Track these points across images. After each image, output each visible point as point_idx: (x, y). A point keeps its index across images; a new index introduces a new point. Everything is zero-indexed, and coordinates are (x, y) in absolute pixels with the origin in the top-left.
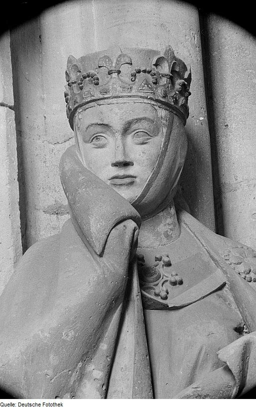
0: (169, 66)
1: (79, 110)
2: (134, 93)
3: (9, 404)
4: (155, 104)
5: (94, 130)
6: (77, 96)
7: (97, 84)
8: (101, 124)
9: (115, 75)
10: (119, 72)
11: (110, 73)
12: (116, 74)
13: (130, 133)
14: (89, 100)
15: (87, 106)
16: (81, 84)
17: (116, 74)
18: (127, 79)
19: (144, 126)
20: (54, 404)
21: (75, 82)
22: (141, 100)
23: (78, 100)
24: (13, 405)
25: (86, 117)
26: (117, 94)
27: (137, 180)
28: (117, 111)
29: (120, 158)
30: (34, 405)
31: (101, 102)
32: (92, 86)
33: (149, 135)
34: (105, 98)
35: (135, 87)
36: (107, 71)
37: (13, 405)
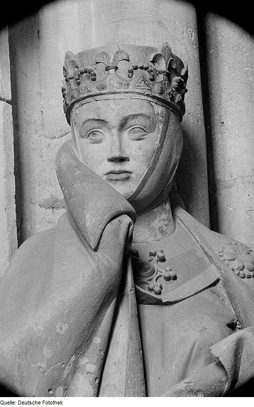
0: (166, 63)
1: (77, 105)
2: (130, 89)
3: (9, 402)
4: (152, 100)
5: (90, 125)
6: (74, 91)
7: (94, 80)
8: (98, 120)
9: (112, 71)
10: (116, 68)
11: (107, 69)
12: (114, 70)
13: (127, 129)
14: (86, 95)
15: (84, 101)
16: (79, 79)
17: (114, 70)
19: (139, 122)
20: (54, 403)
21: (73, 78)
22: (138, 96)
23: (75, 96)
24: (13, 403)
25: (82, 113)
26: (113, 90)
27: (133, 175)
28: (114, 106)
29: (116, 154)
30: (34, 403)
31: (98, 98)
32: (89, 82)
33: (145, 131)
35: (131, 83)
37: (13, 403)
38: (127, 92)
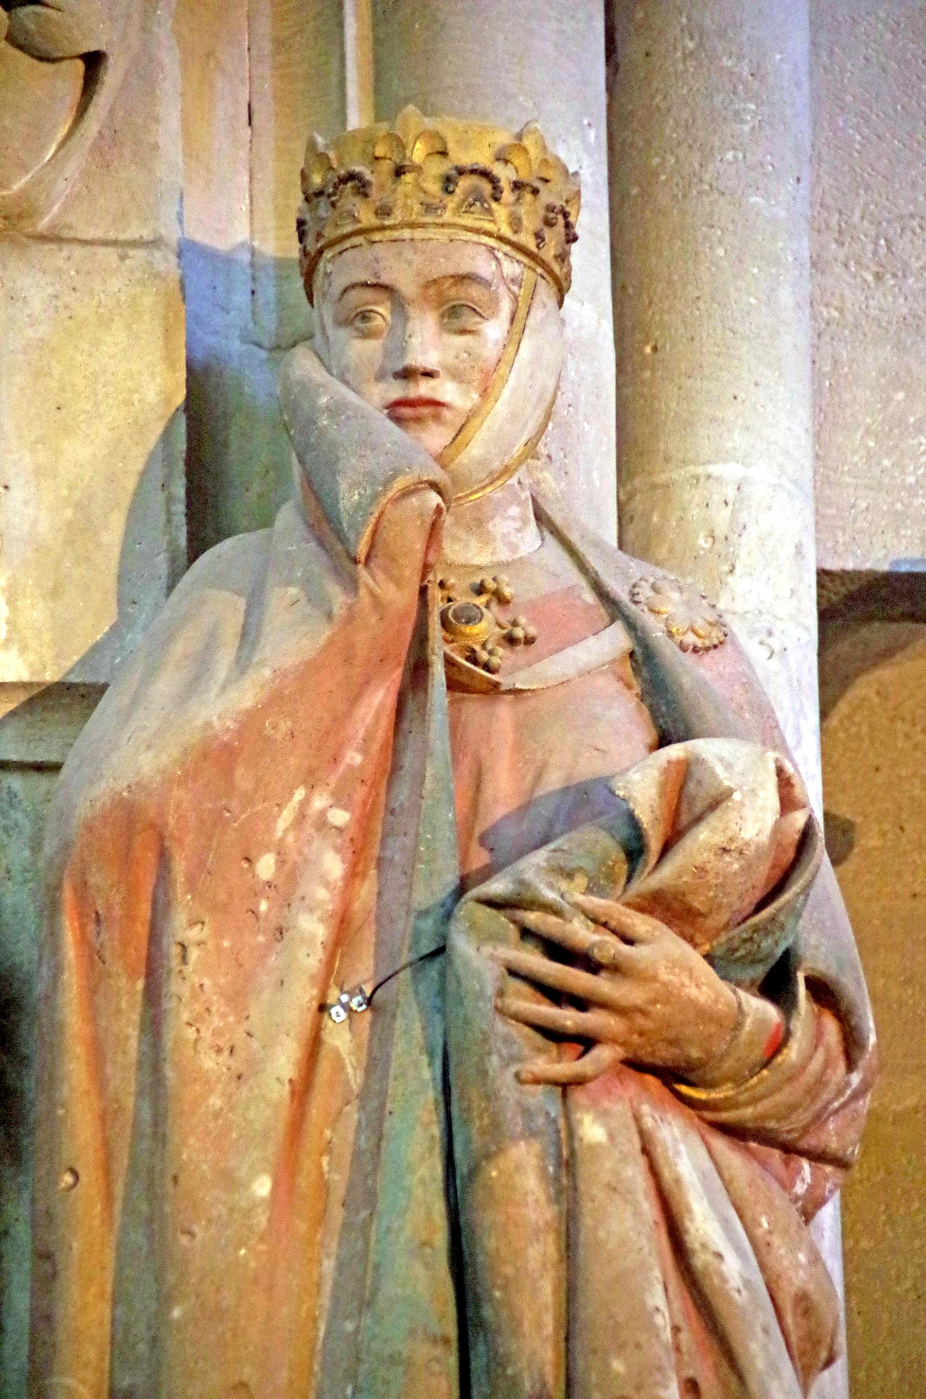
1: (328, 254)
8: (375, 286)
15: (347, 244)
16: (334, 194)
18: (434, 188)
25: (340, 271)
31: (377, 237)
34: (383, 228)
35: (451, 206)
36: (393, 166)
38: (442, 225)
